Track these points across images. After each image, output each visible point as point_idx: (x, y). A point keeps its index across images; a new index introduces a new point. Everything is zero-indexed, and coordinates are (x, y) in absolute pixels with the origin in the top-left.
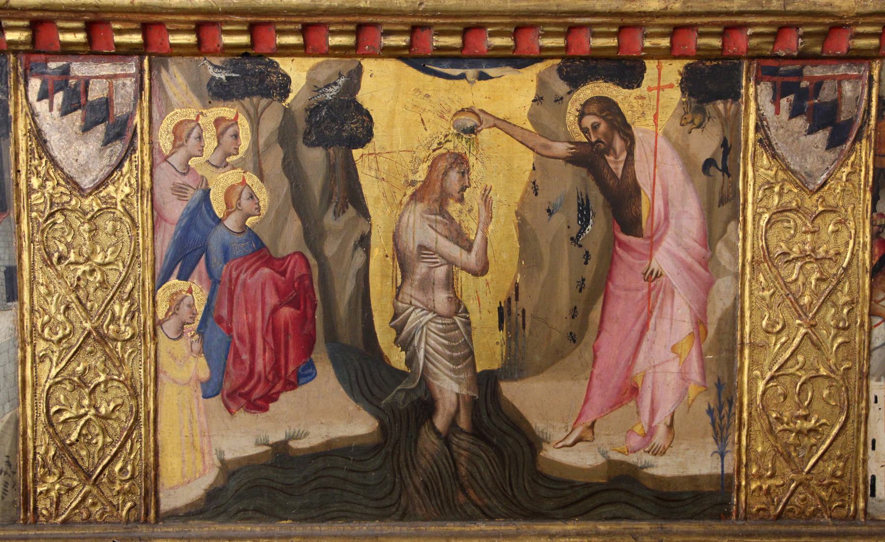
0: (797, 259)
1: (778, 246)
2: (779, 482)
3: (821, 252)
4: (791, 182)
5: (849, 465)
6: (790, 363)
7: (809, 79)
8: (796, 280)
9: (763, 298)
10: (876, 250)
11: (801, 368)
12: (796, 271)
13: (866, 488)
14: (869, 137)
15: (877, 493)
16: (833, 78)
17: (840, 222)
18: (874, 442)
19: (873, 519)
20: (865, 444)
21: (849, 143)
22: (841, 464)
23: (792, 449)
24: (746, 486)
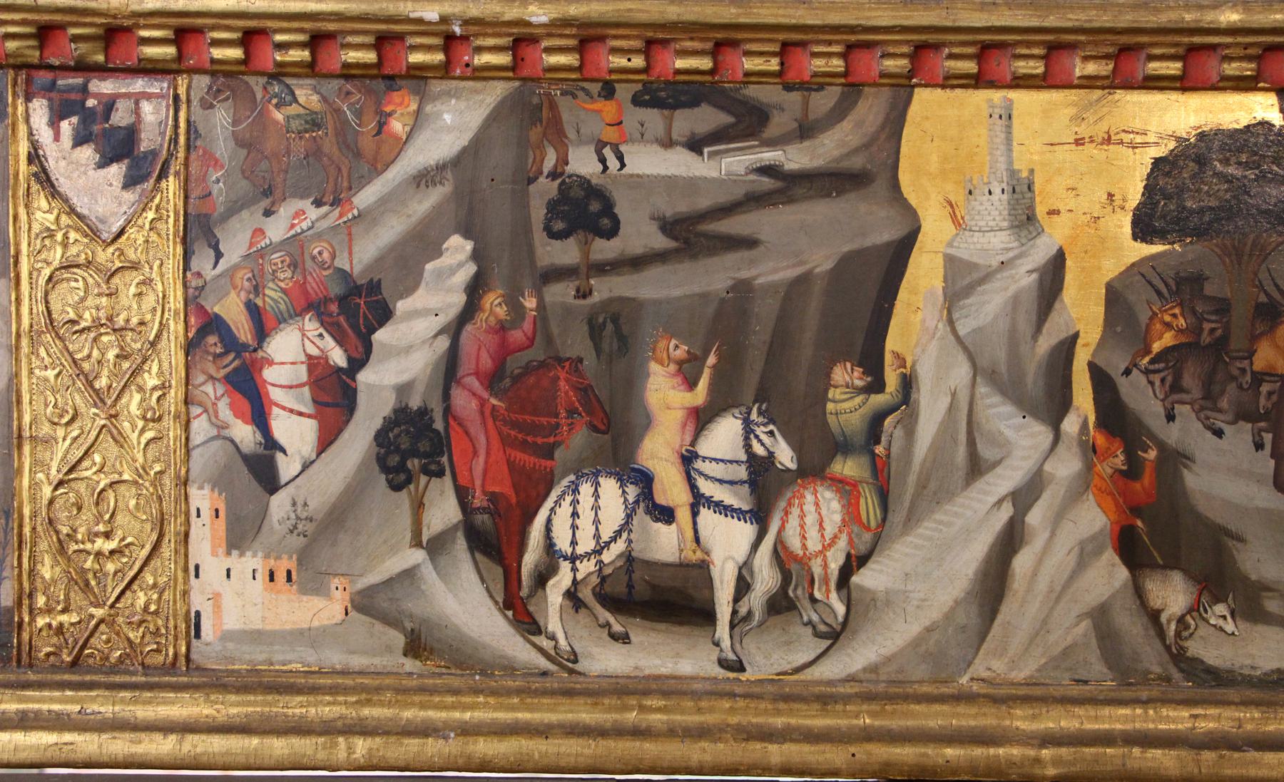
0: (88, 329)
1: (63, 311)
2: (75, 619)
3: (120, 321)
4: (77, 230)
5: (166, 596)
6: (86, 463)
7: (96, 96)
8: (89, 356)
9: (46, 380)
10: (192, 320)
11: (100, 471)
12: (88, 345)
13: (188, 627)
14: (177, 174)
15: (203, 634)
16: (127, 96)
17: (143, 283)
18: (197, 567)
19: (198, 668)
20: (186, 570)
21: (152, 181)
22: (155, 596)
23: (90, 576)
24: (30, 624)
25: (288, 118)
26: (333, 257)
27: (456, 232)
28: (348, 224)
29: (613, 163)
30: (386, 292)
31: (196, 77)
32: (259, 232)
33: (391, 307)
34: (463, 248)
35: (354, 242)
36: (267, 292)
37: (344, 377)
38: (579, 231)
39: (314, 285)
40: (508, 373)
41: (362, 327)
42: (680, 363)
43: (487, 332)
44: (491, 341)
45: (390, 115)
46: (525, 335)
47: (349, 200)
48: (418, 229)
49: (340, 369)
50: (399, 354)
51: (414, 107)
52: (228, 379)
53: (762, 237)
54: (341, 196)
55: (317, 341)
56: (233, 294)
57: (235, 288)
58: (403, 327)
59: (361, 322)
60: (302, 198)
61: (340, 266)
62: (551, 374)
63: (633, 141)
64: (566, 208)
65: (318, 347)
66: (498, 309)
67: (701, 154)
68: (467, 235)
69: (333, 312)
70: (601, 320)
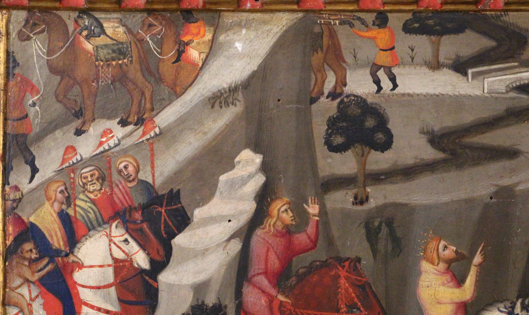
10: (10, 229)
25: (97, 48)
26: (137, 171)
27: (247, 146)
28: (151, 141)
29: (386, 84)
30: (185, 201)
31: (14, 12)
32: (71, 149)
33: (189, 214)
34: (253, 161)
35: (155, 157)
36: (78, 202)
37: (147, 278)
38: (356, 145)
39: (120, 196)
40: (294, 269)
41: (163, 232)
42: (449, 262)
43: (275, 235)
44: (279, 243)
45: (187, 44)
46: (309, 238)
47: (151, 119)
48: (214, 143)
49: (143, 271)
50: (196, 256)
51: (209, 36)
52: (43, 282)
53: (522, 148)
54: (145, 116)
55: (123, 245)
56: (47, 205)
57: (49, 199)
58: (200, 232)
59: (162, 228)
60: (109, 118)
61: (144, 178)
62: (333, 273)
63: (404, 64)
64: (345, 124)
65: (124, 251)
66: (284, 215)
67: (465, 74)
68: (256, 149)
69: (137, 220)
70: (376, 224)
